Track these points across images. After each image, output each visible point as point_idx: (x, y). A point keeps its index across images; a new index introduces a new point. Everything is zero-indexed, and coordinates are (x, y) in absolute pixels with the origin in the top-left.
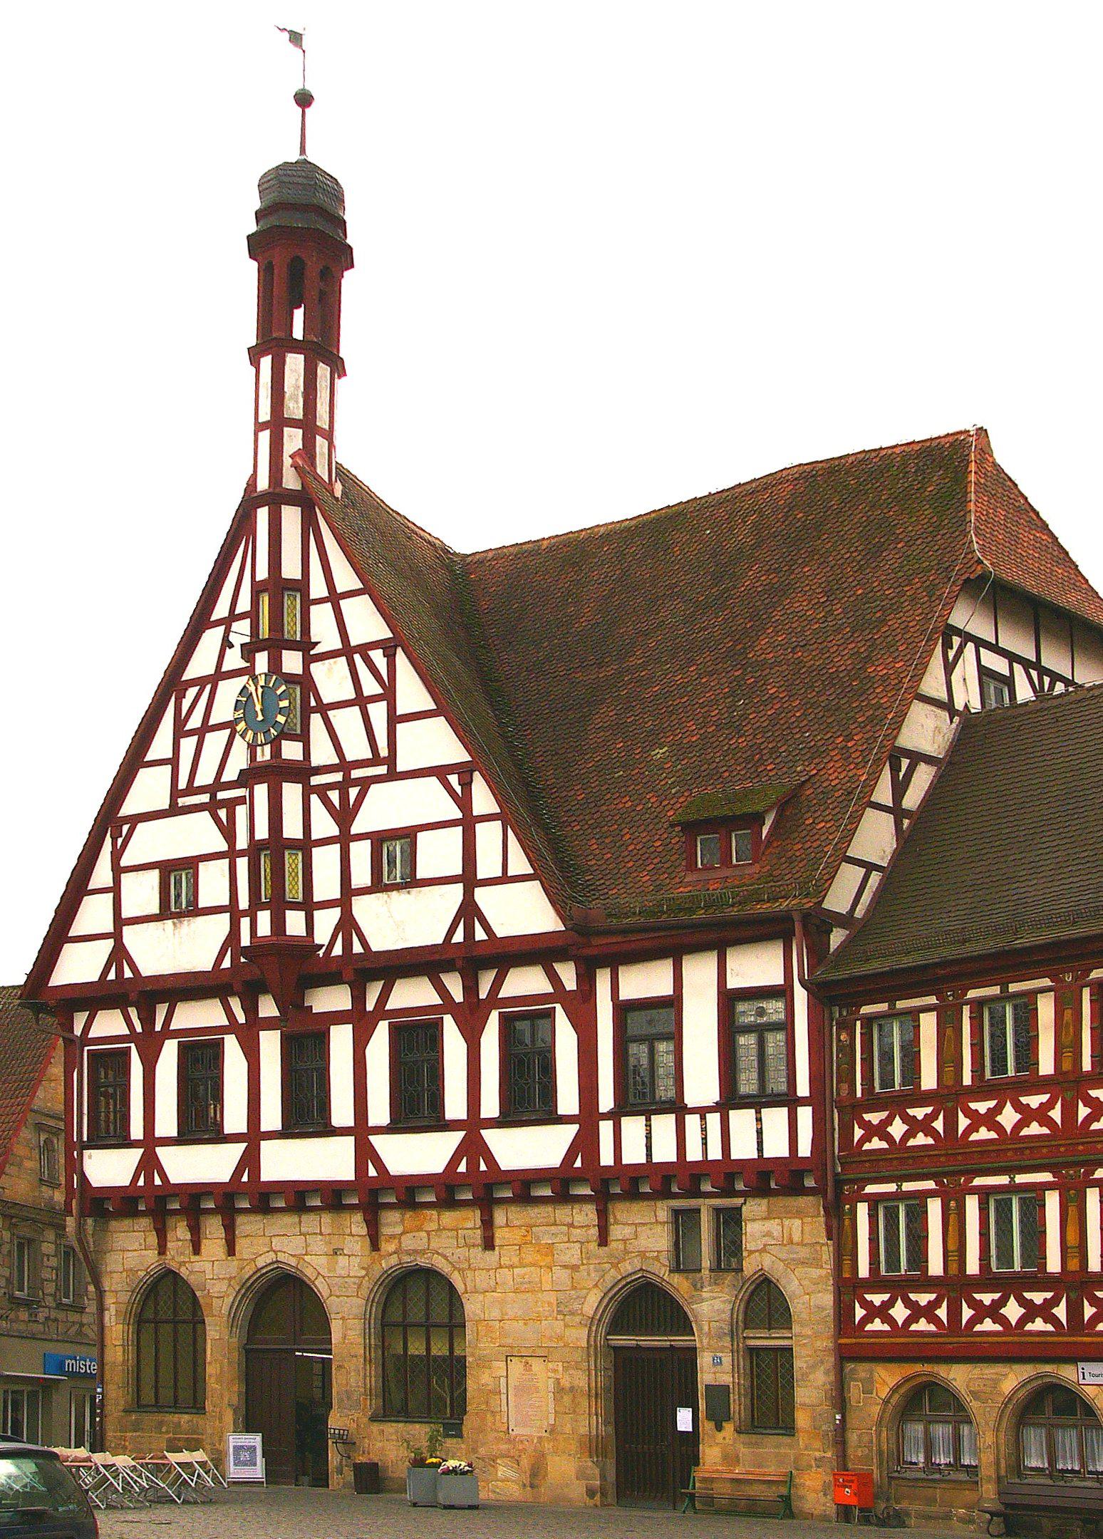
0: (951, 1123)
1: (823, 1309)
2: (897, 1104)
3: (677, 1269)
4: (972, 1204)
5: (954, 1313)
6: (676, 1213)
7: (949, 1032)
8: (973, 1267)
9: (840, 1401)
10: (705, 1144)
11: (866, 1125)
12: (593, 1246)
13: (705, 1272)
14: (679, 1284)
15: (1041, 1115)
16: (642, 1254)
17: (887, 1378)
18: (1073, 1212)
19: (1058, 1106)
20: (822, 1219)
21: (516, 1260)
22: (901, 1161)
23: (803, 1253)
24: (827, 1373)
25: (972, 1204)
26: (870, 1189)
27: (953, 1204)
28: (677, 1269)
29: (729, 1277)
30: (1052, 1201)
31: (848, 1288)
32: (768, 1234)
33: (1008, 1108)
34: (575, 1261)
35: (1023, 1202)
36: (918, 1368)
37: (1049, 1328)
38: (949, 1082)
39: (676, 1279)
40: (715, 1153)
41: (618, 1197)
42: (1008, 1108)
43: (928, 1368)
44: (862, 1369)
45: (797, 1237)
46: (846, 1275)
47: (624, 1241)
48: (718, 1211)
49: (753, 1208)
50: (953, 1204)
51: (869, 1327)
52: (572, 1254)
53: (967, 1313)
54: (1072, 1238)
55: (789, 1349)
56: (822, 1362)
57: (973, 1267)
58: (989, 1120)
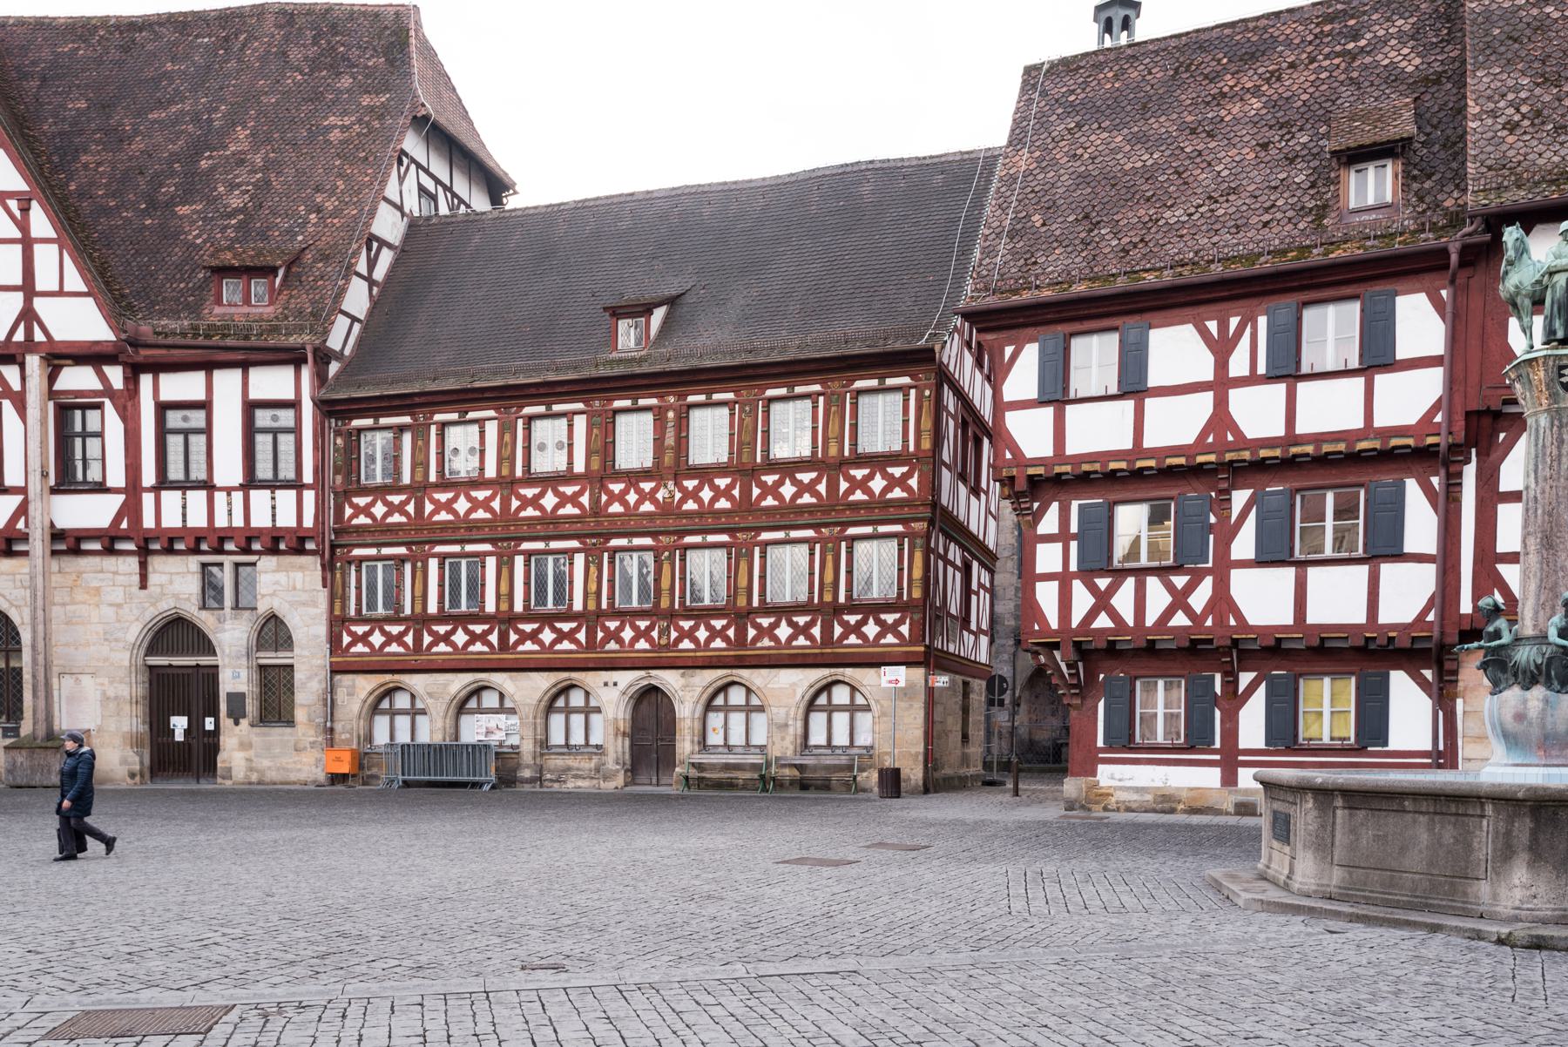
0: (420, 508)
2: (380, 492)
3: (204, 607)
6: (204, 565)
8: (433, 608)
10: (230, 513)
11: (354, 506)
12: (135, 589)
13: (227, 610)
14: (205, 620)
16: (176, 596)
21: (67, 599)
23: (304, 597)
25: (433, 564)
26: (357, 552)
28: (204, 607)
29: (247, 614)
30: (491, 562)
32: (277, 583)
33: (462, 498)
34: (120, 600)
35: (468, 564)
39: (204, 615)
40: (238, 522)
41: (155, 552)
42: (462, 498)
45: (299, 586)
46: (337, 613)
47: (161, 586)
48: (237, 565)
49: (267, 563)
52: (117, 595)
54: (504, 589)
57: (433, 608)
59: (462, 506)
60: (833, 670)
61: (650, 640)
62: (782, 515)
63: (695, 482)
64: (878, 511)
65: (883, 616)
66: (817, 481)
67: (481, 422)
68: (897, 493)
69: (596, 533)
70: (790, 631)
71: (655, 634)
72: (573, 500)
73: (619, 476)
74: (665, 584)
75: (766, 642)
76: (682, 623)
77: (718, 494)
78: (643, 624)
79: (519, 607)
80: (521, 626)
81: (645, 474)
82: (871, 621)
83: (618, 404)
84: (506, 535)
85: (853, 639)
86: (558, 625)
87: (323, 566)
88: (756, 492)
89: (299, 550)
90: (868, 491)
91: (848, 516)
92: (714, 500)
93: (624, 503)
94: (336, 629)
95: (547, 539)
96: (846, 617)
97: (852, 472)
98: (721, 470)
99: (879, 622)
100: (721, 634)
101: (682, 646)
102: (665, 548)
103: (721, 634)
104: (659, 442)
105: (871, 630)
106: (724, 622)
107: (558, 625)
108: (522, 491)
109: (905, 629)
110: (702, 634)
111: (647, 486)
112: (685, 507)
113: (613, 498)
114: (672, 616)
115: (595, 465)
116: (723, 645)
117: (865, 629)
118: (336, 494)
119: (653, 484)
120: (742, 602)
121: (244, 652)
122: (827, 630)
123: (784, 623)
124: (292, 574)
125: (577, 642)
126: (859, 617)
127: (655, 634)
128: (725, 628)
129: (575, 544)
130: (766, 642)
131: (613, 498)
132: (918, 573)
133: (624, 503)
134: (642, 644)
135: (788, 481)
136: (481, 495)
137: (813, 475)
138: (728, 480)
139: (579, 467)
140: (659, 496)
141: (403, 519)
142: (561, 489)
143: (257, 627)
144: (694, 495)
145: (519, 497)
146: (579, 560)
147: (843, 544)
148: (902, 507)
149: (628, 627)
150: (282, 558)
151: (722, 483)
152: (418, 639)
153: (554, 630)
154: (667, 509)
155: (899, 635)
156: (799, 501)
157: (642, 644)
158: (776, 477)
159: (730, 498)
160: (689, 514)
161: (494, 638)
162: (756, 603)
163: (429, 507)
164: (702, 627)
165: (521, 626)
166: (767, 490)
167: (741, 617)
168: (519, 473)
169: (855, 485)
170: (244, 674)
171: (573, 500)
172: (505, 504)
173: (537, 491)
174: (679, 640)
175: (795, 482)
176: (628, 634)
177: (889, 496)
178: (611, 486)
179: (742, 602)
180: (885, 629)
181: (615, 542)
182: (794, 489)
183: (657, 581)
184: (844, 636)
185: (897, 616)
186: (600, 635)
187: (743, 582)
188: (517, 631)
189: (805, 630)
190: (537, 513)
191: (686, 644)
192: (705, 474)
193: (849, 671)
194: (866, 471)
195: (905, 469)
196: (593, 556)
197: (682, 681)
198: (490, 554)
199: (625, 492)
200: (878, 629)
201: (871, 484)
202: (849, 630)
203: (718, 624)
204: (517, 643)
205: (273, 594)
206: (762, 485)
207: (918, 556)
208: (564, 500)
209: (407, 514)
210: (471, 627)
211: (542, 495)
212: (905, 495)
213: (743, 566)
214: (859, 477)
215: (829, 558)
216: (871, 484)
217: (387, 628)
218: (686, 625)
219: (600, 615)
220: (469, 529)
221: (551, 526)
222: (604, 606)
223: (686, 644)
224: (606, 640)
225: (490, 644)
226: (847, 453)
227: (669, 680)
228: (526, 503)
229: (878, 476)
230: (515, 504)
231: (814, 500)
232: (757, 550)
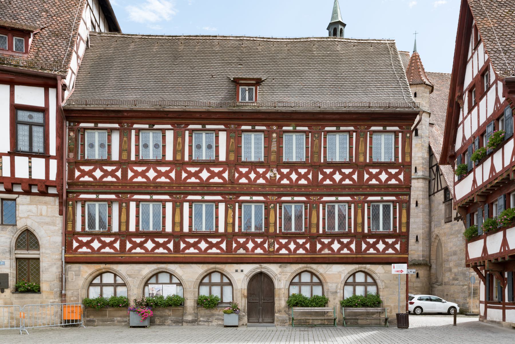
0: (125, 174)
1: (57, 243)
4: (133, 205)
5: (123, 245)
7: (125, 139)
8: (132, 228)
9: (63, 280)
15: (166, 174)
17: (87, 270)
18: (178, 211)
19: (174, 172)
20: (58, 207)
22: (99, 187)
23: (48, 220)
24: (57, 268)
25: (133, 205)
26: (82, 196)
27: (124, 204)
30: (169, 206)
31: (69, 235)
36: (102, 266)
37: (166, 251)
38: (125, 157)
43: (108, 266)
44: (75, 267)
45: (44, 213)
46: (70, 229)
50: (124, 204)
51: (80, 250)
53: (129, 245)
54: (177, 219)
55: (39, 259)
56: (55, 264)
57: (132, 228)
58: (143, 174)
59: (152, 174)
60: (360, 266)
61: (263, 248)
62: (334, 189)
63: (288, 170)
64: (384, 189)
65: (387, 240)
66: (352, 173)
67: (163, 131)
68: (393, 182)
69: (231, 193)
70: (339, 246)
71: (266, 245)
72: (219, 175)
73: (244, 164)
74: (272, 220)
75: (326, 251)
76: (281, 240)
77: (300, 176)
78: (259, 241)
79: (186, 229)
80: (187, 240)
81: (260, 164)
82: (381, 242)
83: (243, 127)
84: (178, 192)
85: (372, 251)
86: (210, 240)
87: (61, 204)
88: (321, 177)
89: (44, 193)
90: (379, 180)
91: (368, 191)
92: (298, 180)
93: (248, 178)
94: (69, 239)
95: (203, 194)
96: (368, 240)
97: (371, 170)
98: (302, 165)
99: (384, 243)
100: (303, 246)
101: (281, 252)
102: (272, 202)
103: (303, 246)
104: (267, 149)
105: (381, 246)
106: (304, 240)
107: (210, 240)
108: (189, 169)
109: (398, 246)
110: (292, 246)
111: (261, 171)
112: (282, 182)
113: (241, 175)
114: (276, 236)
115: (232, 157)
116: (304, 252)
117: (377, 246)
118: (69, 163)
119: (264, 170)
120: (314, 231)
121: (8, 250)
122: (359, 246)
123: (336, 242)
124: (39, 207)
125: (221, 249)
126: (375, 240)
127: (266, 245)
128: (304, 244)
129: (219, 198)
130: (326, 251)
131: (241, 175)
132: (404, 220)
133: (248, 178)
134: (259, 251)
135: (337, 173)
136: (163, 169)
137: (351, 170)
138: (306, 170)
139: (222, 158)
140: (268, 176)
141: (114, 180)
142: (212, 169)
143: (16, 236)
144: (287, 176)
145: (186, 172)
146: (222, 207)
147: (366, 205)
148: (395, 188)
149: (250, 242)
150: (33, 197)
151: (303, 171)
152: (123, 245)
153: (207, 242)
154: (271, 182)
155: (395, 249)
156: (344, 183)
157: (259, 251)
158: (331, 170)
159: (307, 179)
160: (285, 186)
161: (171, 246)
162: (321, 231)
163: (130, 174)
164: (292, 243)
165: (187, 240)
166: (326, 176)
167: (313, 238)
168: (187, 159)
169: (372, 176)
170: (7, 263)
171: (219, 175)
172: (178, 175)
173: (197, 169)
174: (279, 249)
175: (341, 173)
176: (250, 245)
177: (389, 183)
178: (241, 169)
179: (314, 231)
180: (388, 246)
181: (242, 198)
182: (341, 177)
183: (267, 219)
184: (367, 249)
185: (394, 240)
186: (234, 245)
187: (314, 221)
188: (185, 242)
189: (347, 246)
190: (198, 181)
191: (284, 251)
192: (293, 166)
193: (368, 266)
194: (378, 170)
195: (397, 170)
196: (230, 205)
197: (279, 270)
198: (169, 201)
199: (249, 172)
200: (384, 246)
201: (380, 176)
202: (369, 246)
203: (301, 241)
204: (185, 249)
205: (28, 217)
206: (324, 174)
207: (404, 212)
208: (213, 175)
209: (116, 177)
210: (157, 240)
211: (200, 171)
212: (397, 182)
213: (314, 213)
214: (374, 173)
215: (360, 211)
216: (380, 176)
217: (103, 239)
218: (284, 241)
219: (235, 235)
220: (156, 187)
221: (205, 188)
222: (237, 230)
223: (284, 251)
224: (238, 248)
225: (168, 249)
226: (368, 161)
227: (273, 269)
228: (190, 175)
229: (384, 173)
230: (184, 175)
231: (351, 183)
232: (321, 206)
